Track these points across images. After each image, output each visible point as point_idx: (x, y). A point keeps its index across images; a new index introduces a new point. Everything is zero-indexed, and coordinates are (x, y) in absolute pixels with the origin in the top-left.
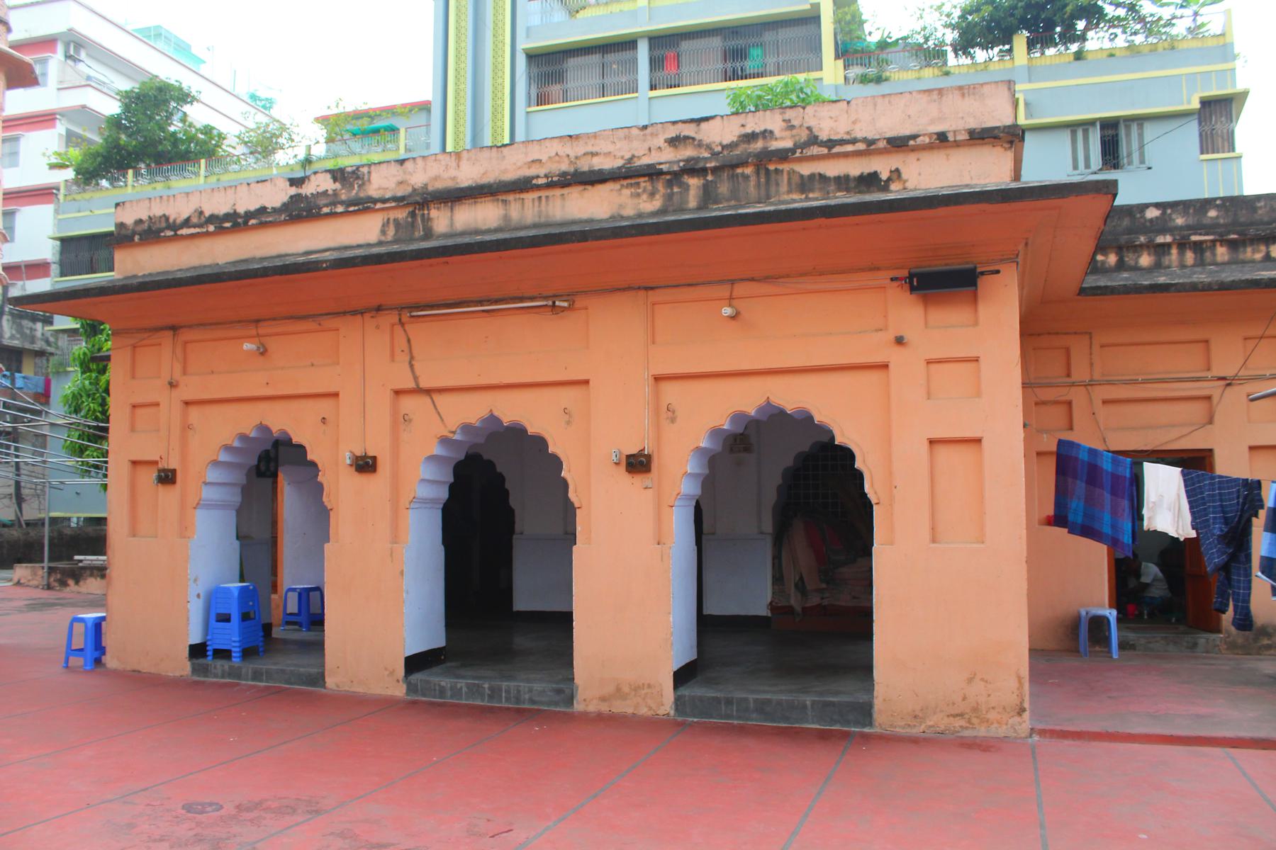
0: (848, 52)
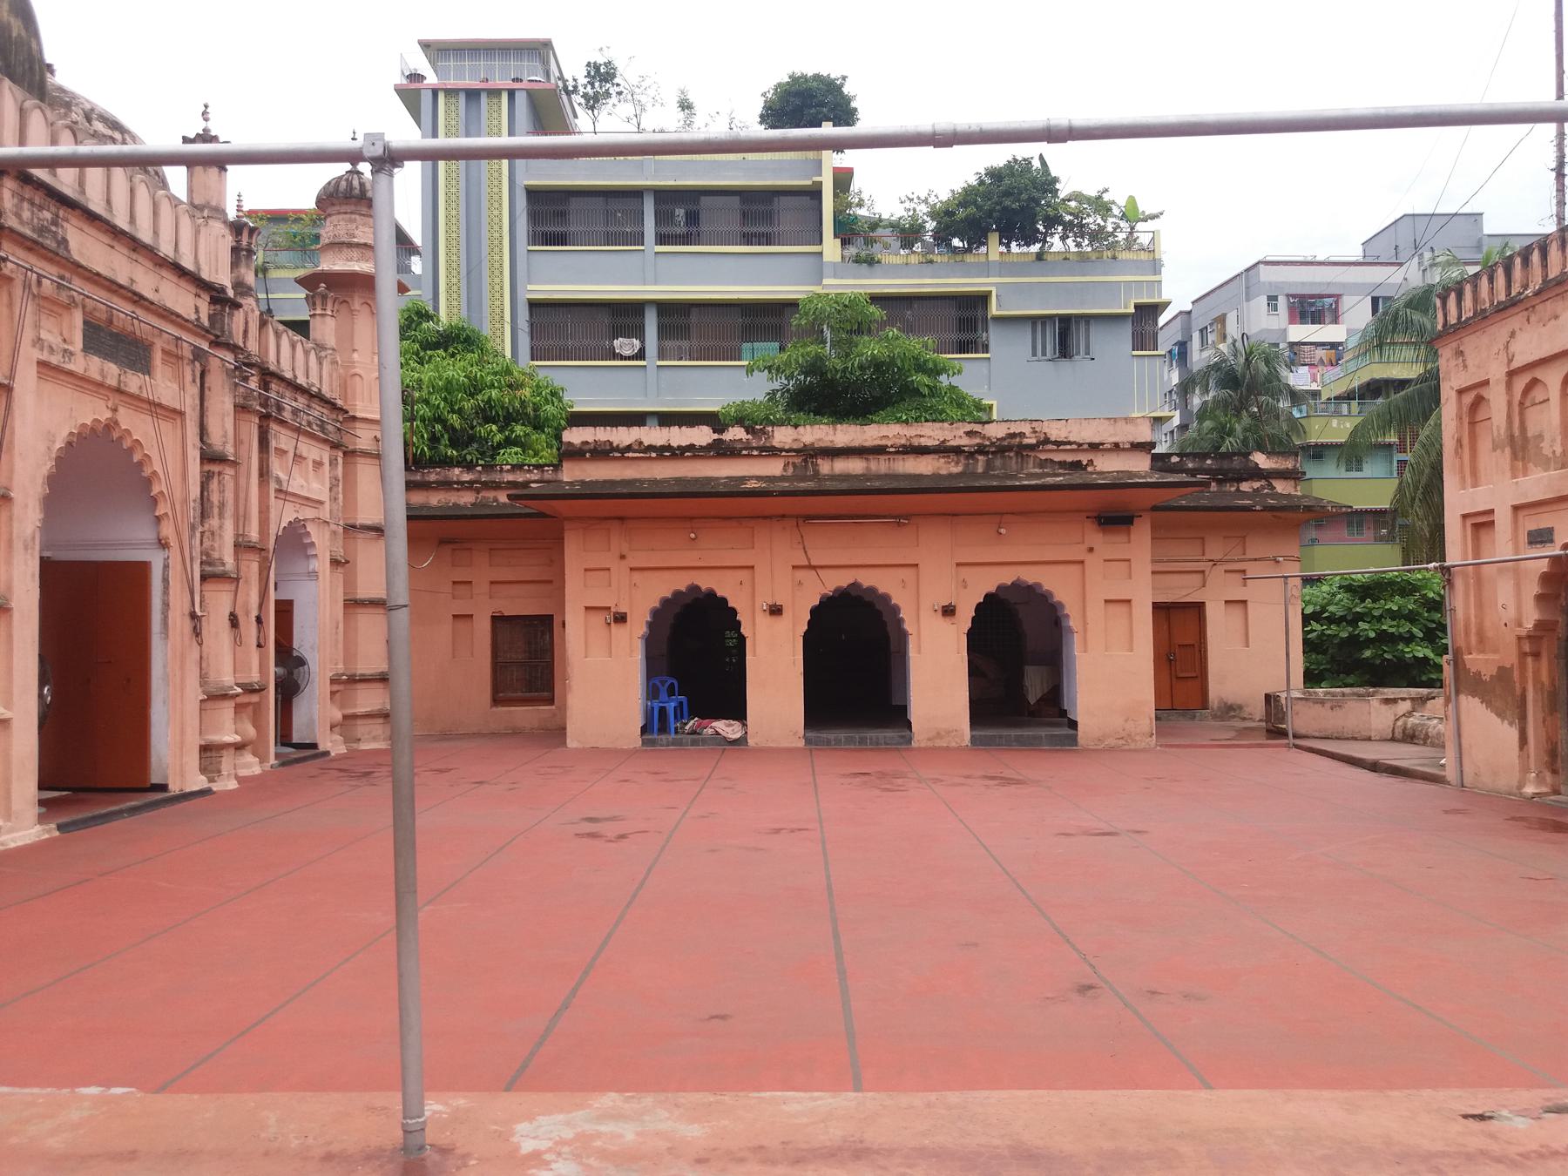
0: (848, 230)
